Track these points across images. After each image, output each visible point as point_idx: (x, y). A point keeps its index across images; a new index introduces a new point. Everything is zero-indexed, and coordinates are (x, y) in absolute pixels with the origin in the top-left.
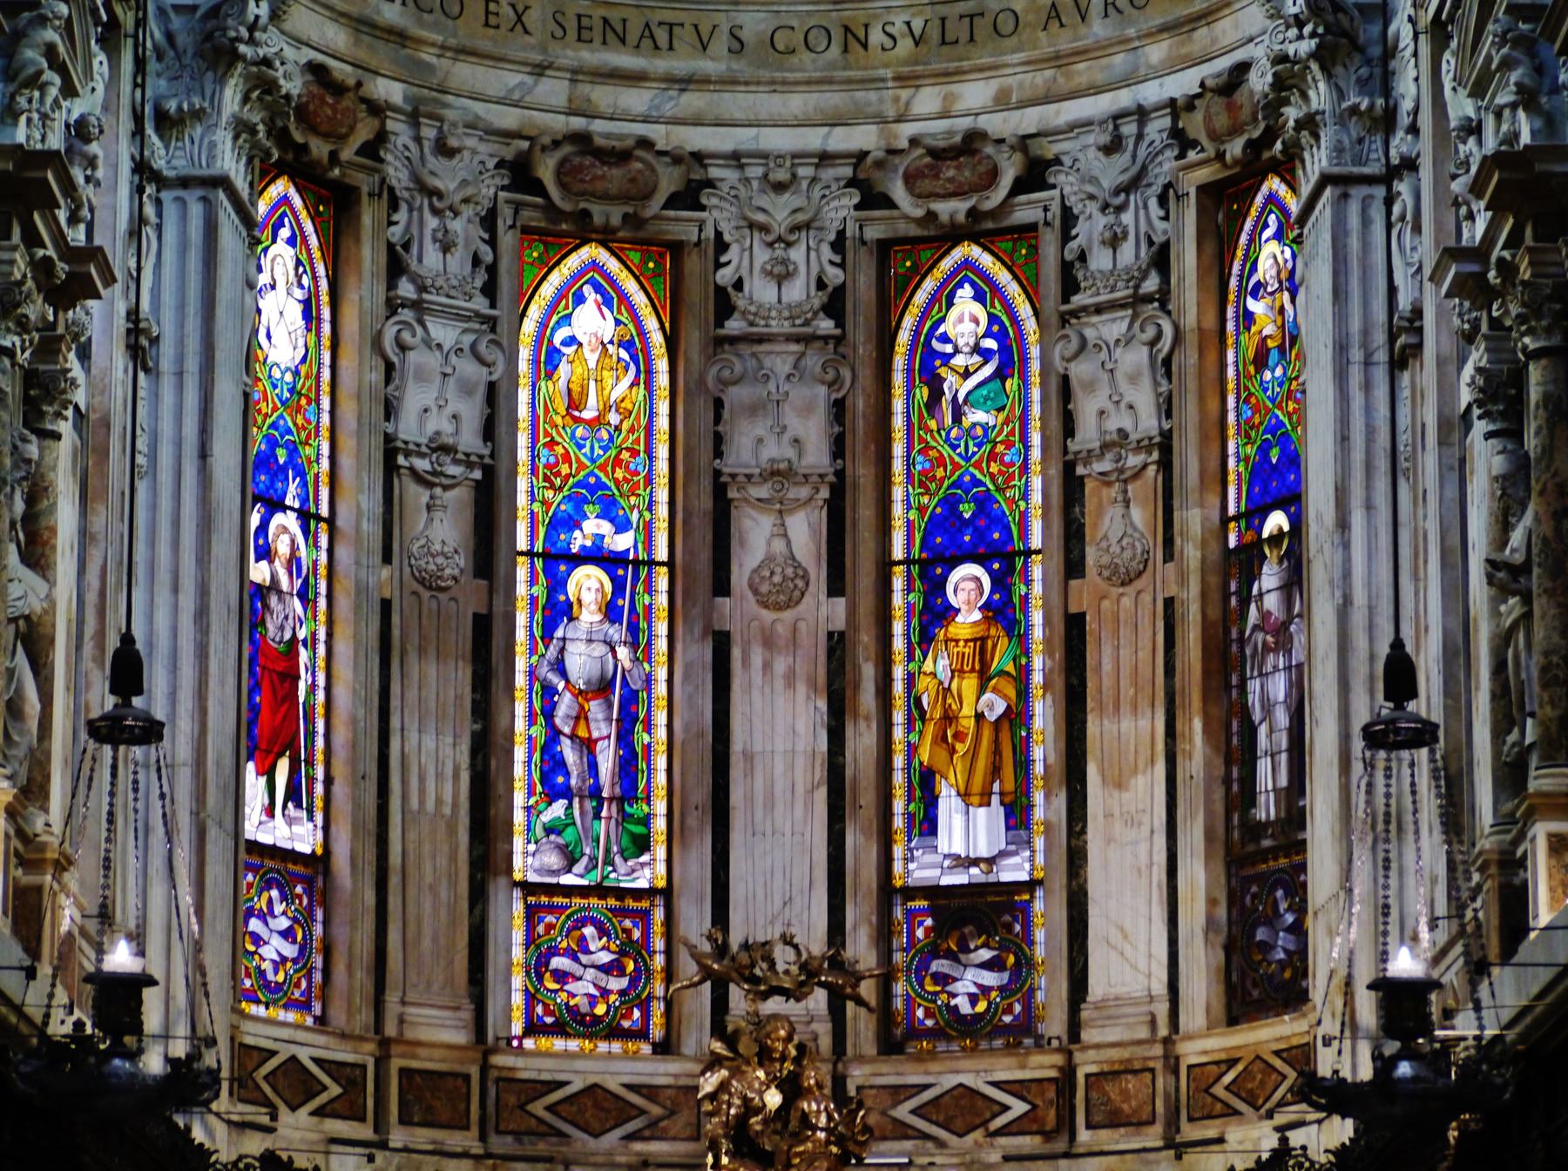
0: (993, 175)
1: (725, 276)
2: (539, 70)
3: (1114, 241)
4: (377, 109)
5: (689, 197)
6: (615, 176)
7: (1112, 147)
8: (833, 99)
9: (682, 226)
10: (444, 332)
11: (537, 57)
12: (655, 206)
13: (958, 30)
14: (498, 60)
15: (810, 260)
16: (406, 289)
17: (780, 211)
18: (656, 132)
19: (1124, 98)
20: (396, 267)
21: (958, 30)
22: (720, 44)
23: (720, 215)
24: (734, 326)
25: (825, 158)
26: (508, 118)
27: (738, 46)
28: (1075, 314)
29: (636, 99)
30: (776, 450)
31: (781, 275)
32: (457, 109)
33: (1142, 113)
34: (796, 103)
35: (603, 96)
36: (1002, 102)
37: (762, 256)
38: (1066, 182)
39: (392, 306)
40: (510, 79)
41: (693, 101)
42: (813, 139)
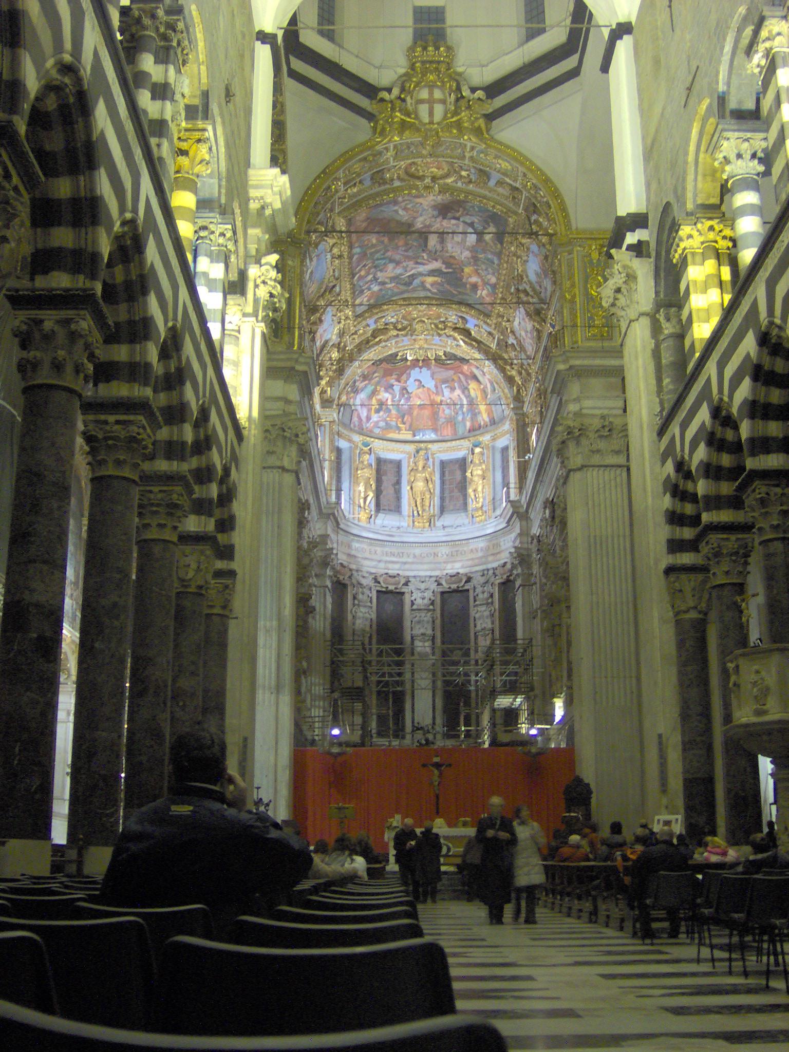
0: (461, 581)
1: (413, 598)
2: (380, 561)
3: (483, 593)
4: (351, 570)
5: (406, 584)
6: (393, 580)
7: (483, 575)
8: (432, 566)
9: (404, 589)
10: (363, 610)
11: (379, 559)
12: (400, 586)
13: (455, 554)
14: (372, 560)
15: (428, 595)
16: (356, 602)
17: (423, 586)
18: (401, 573)
19: (484, 567)
20: (354, 598)
21: (455, 554)
22: (412, 556)
23: (411, 587)
24: (415, 607)
25: (431, 577)
26: (373, 571)
27: (415, 556)
28: (477, 606)
29: (397, 566)
30: (422, 631)
31: (423, 599)
32: (365, 569)
33: (488, 570)
34: (426, 567)
35: (390, 566)
36: (462, 567)
37: (420, 595)
38: (474, 582)
39: (354, 605)
40: (374, 563)
41: (407, 566)
42: (428, 573)
